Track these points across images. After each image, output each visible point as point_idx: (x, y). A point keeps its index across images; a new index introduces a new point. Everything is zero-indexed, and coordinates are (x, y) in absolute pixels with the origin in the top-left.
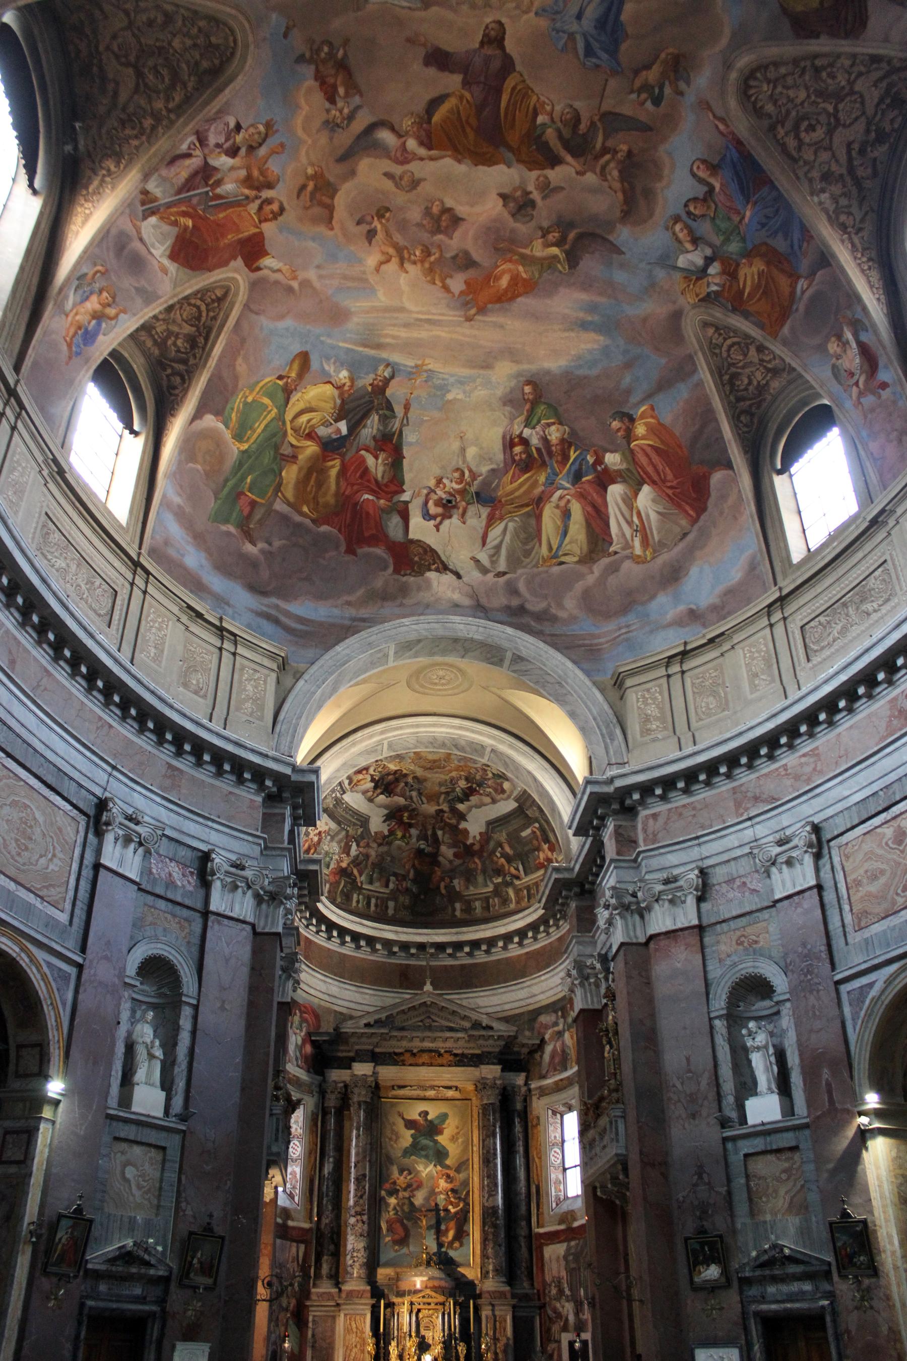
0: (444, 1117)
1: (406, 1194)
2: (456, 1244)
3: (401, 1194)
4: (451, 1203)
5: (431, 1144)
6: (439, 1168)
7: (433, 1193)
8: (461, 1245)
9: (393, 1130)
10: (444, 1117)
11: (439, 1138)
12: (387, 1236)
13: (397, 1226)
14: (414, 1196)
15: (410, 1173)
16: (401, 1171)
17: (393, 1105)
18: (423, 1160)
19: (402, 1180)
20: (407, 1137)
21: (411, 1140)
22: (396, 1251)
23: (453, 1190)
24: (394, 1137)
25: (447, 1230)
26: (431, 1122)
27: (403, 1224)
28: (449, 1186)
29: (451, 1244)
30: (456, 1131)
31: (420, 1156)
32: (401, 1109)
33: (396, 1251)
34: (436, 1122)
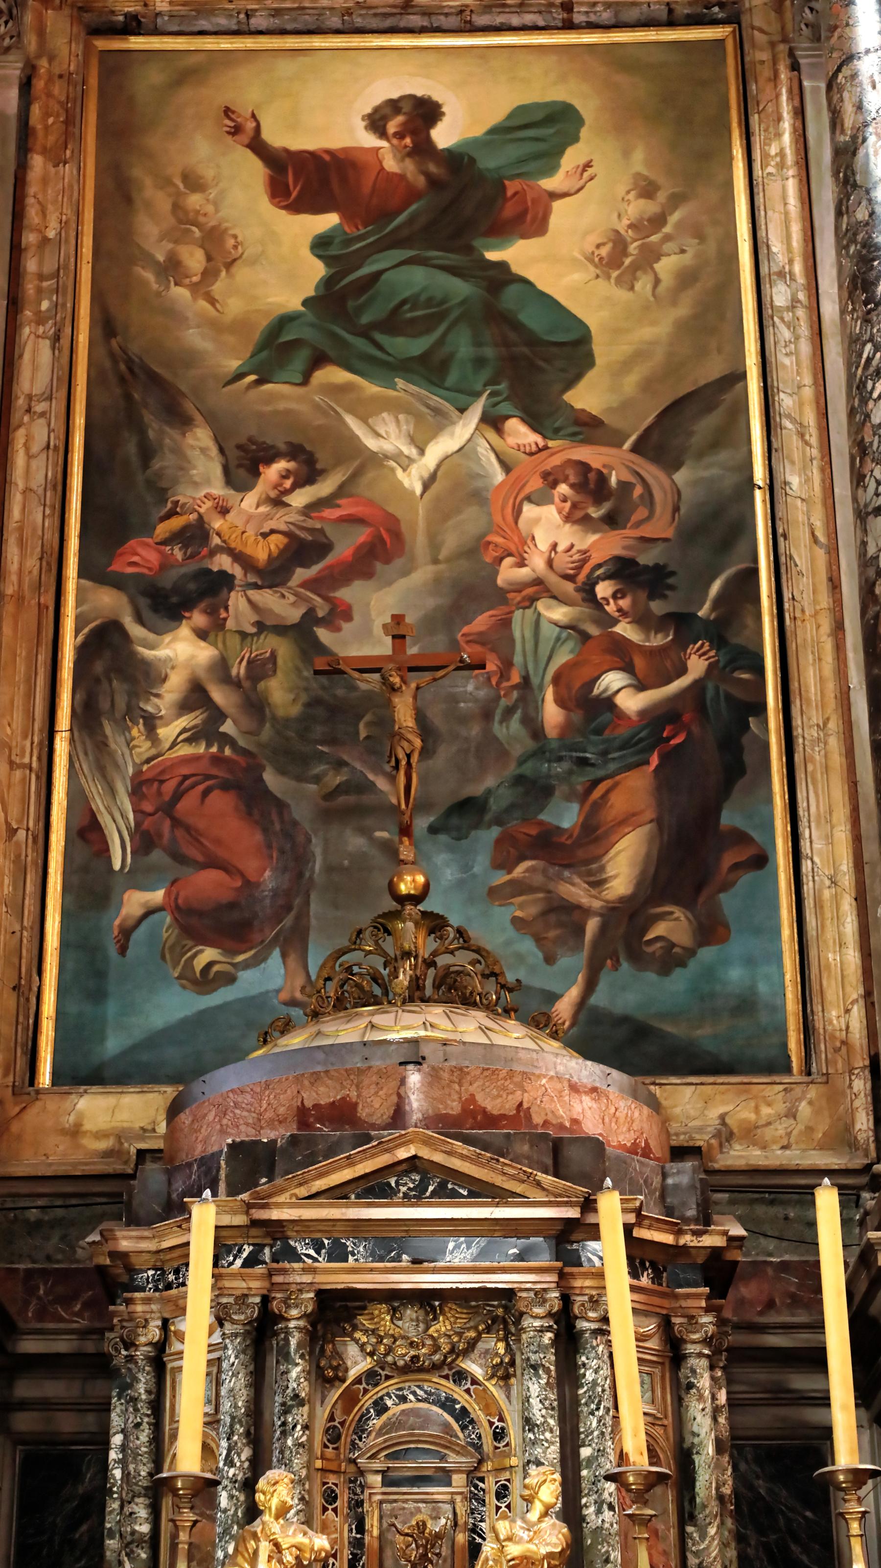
0: (546, 129)
1: (283, 606)
2: (672, 926)
3: (239, 607)
4: (621, 655)
5: (461, 289)
6: (520, 434)
7: (473, 589)
8: (711, 930)
9: (184, 220)
10: (546, 129)
11: (517, 255)
12: (137, 877)
13: (219, 816)
14: (340, 613)
15: (309, 474)
16: (244, 462)
17: (188, 73)
18: (403, 388)
19: (249, 518)
20: (282, 260)
21: (318, 270)
22: (207, 981)
23: (623, 570)
24: (194, 260)
25: (594, 836)
26: (457, 161)
27: (255, 800)
28: (602, 545)
29: (627, 923)
30: (637, 208)
31: (385, 368)
32: (247, 92)
33: (207, 981)
34: (488, 162)
